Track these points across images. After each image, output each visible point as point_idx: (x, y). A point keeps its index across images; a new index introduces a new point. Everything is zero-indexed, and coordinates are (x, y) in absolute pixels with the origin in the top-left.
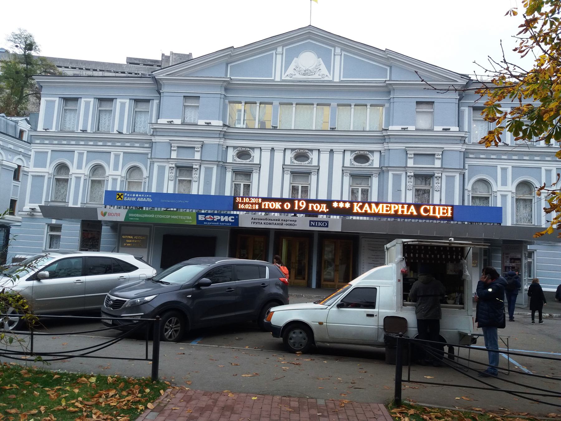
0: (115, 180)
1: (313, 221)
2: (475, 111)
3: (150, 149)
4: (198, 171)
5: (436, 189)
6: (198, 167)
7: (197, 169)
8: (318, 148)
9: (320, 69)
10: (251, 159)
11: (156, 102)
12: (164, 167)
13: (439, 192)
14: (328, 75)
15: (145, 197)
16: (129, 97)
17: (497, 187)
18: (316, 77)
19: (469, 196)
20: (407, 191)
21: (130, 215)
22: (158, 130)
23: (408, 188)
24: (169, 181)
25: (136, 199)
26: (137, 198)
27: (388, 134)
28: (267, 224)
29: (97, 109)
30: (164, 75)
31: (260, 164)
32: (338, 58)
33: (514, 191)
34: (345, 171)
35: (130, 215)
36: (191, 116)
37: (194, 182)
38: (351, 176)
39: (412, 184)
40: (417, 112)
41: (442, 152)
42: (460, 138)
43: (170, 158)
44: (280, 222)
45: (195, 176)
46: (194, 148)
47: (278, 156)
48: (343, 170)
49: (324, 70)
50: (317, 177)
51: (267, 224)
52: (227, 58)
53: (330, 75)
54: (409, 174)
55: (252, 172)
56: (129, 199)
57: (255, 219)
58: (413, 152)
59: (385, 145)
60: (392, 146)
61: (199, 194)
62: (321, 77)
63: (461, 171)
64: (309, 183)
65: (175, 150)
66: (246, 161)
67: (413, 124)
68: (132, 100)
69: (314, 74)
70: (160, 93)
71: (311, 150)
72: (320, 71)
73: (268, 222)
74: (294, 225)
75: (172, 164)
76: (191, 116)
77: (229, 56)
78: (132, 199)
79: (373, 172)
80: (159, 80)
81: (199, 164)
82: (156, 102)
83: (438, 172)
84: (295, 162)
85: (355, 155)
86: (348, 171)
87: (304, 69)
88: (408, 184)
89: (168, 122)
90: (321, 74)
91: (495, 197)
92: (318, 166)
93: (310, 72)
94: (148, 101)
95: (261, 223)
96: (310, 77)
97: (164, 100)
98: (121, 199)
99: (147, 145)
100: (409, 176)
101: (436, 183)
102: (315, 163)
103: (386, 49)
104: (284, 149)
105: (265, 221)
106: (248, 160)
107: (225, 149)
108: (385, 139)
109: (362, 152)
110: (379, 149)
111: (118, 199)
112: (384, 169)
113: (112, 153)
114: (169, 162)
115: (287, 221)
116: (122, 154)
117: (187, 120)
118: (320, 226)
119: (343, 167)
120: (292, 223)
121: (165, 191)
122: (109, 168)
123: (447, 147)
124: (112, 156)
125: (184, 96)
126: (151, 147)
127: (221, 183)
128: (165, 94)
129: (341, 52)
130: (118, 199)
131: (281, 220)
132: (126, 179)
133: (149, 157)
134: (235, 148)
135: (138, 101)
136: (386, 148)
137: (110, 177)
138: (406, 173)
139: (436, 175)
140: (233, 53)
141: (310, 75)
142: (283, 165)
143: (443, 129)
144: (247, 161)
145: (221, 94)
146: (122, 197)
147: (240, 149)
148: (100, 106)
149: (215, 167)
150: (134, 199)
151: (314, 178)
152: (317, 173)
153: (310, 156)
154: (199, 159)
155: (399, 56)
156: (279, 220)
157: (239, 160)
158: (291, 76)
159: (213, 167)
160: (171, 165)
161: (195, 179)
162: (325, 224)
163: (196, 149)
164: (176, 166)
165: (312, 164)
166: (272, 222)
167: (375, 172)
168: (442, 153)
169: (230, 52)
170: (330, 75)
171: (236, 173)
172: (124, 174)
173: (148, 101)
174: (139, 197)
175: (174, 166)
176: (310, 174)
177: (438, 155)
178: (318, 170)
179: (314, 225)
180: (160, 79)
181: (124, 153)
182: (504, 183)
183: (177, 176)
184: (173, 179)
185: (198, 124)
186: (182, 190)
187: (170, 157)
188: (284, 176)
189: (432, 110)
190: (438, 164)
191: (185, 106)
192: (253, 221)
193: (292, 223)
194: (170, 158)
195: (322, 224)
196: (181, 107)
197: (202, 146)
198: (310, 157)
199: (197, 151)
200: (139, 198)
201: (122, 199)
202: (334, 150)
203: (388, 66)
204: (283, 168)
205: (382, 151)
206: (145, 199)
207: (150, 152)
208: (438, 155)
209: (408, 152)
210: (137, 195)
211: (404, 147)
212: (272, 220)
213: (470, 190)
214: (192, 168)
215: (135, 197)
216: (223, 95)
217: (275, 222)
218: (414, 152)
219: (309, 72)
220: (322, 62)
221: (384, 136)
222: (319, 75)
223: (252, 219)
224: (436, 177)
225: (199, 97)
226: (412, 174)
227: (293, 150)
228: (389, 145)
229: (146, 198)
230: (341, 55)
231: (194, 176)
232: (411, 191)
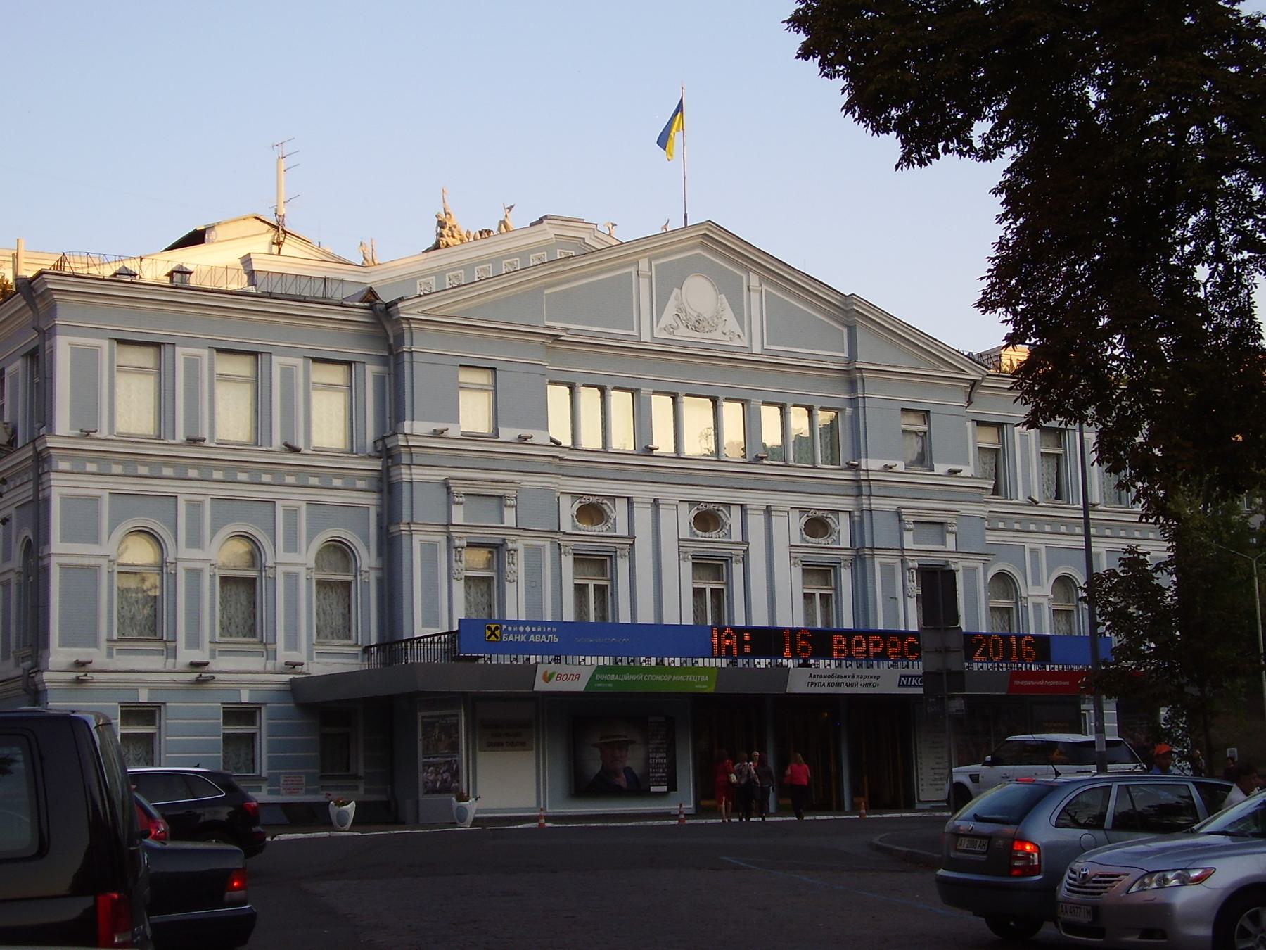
15: (544, 633)
105: (831, 680)
146: (497, 633)
156: (853, 677)
167: (845, 557)
192: (811, 680)
193: (874, 680)
210: (528, 629)
223: (811, 676)
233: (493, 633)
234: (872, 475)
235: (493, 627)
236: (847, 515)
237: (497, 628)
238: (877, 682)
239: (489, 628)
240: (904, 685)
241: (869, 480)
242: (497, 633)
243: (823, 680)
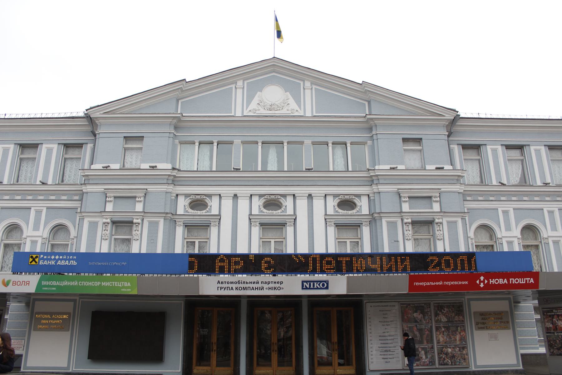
0: (34, 243)
1: (307, 282)
2: (466, 150)
3: (80, 202)
4: (140, 226)
5: (438, 238)
6: (139, 221)
7: (139, 224)
8: (293, 192)
9: (288, 104)
10: (207, 209)
11: (90, 146)
12: (96, 223)
13: (442, 241)
14: (298, 109)
16: (58, 141)
17: (501, 232)
18: (284, 112)
19: (472, 244)
20: (406, 241)
22: (90, 177)
23: (406, 238)
24: (102, 240)
25: (56, 263)
27: (377, 174)
28: (240, 289)
29: (18, 157)
30: (101, 113)
31: (219, 215)
32: (308, 92)
33: (520, 236)
34: (329, 220)
35: (44, 283)
36: (132, 160)
37: (134, 241)
38: (336, 226)
39: (410, 232)
40: (405, 150)
41: (439, 194)
42: (456, 178)
43: (105, 212)
44: (260, 285)
45: (136, 233)
46: (135, 197)
47: (243, 204)
48: (325, 219)
49: (293, 105)
50: (294, 229)
51: (240, 289)
52: (178, 93)
53: (301, 109)
54: (405, 221)
55: (209, 226)
56: (46, 263)
58: (407, 195)
59: (374, 187)
60: (382, 188)
61: (141, 253)
62: (290, 113)
63: (463, 215)
64: (284, 237)
65: (111, 201)
66: (202, 212)
67: (402, 164)
68: (61, 145)
69: (282, 109)
70: (95, 135)
71: (284, 196)
72: (288, 105)
74: (279, 288)
75: (107, 219)
76: (132, 160)
77: (180, 90)
78: (50, 263)
79: (362, 220)
80: (95, 120)
81: (141, 217)
82: (90, 146)
83: (438, 217)
84: (265, 211)
85: (339, 201)
86: (332, 220)
87: (270, 103)
88: (406, 233)
89: (103, 167)
90: (290, 109)
91: (500, 245)
92: (295, 214)
93: (277, 107)
94: (79, 146)
95: (232, 289)
96: (278, 113)
97: (100, 142)
98: (35, 263)
99: (77, 198)
100: (406, 223)
101: (438, 230)
102: (290, 211)
103: (363, 81)
104: (249, 195)
106: (204, 211)
107: (174, 198)
108: (373, 181)
109: (347, 197)
110: (367, 193)
111: (31, 263)
112: (375, 215)
113: (32, 209)
114: (103, 216)
115: (269, 283)
116: (45, 210)
117: (127, 166)
118: (317, 288)
119: (326, 215)
120: (277, 285)
121: (97, 251)
122: (28, 228)
123: (444, 188)
124: (33, 213)
125: (124, 137)
126: (81, 200)
127: (170, 238)
128: (101, 135)
129: (311, 85)
130: (31, 263)
131: (260, 283)
132: (49, 241)
133: (79, 211)
134: (187, 196)
135: (69, 147)
136: (375, 190)
137: (28, 239)
138: (402, 220)
139: (437, 221)
140: (184, 88)
141: (277, 110)
142: (249, 215)
143: (391, 168)
144: (203, 212)
145: (170, 133)
147: (194, 198)
148: (22, 153)
149: (162, 220)
150: (53, 263)
151: (290, 230)
152: (294, 224)
153: (282, 202)
154: (141, 210)
155: (378, 90)
156: (258, 283)
157: (193, 211)
158: (255, 111)
159: (159, 221)
160: (105, 220)
161: (136, 238)
162: (323, 285)
163: (137, 199)
164: (111, 221)
165: (286, 213)
167: (365, 220)
168: (440, 195)
169: (182, 86)
170: (301, 109)
171: (189, 227)
172: (46, 235)
173: (79, 146)
174: (59, 259)
175: (109, 221)
176: (285, 225)
177: (435, 197)
178: (295, 219)
179: (308, 286)
180: (96, 118)
181: (48, 208)
182: (508, 228)
183: (113, 234)
184: (107, 238)
185: (141, 168)
186: (121, 249)
187: (105, 210)
188: (251, 229)
189: (420, 148)
190: (436, 207)
191: (126, 149)
193: (277, 285)
194: (105, 212)
195: (319, 285)
196: (121, 151)
197: (145, 194)
198: (284, 204)
199: (138, 201)
202: (313, 195)
203: (366, 101)
204: (250, 219)
205: (370, 195)
206: (67, 261)
207: (80, 205)
208: (435, 197)
209: (401, 194)
211: (397, 189)
212: (247, 283)
213: (472, 238)
214: (132, 222)
215: (55, 259)
216: (172, 134)
217: (251, 286)
218: (407, 194)
219: (276, 107)
220: (290, 96)
221: (371, 176)
222: (288, 110)
224: (437, 223)
225: (143, 137)
226: (410, 221)
227: (261, 196)
228: (379, 187)
229: (69, 260)
230: (312, 89)
231: (134, 233)
232: (411, 241)
233: (34, 260)
234: (378, 172)
235: (34, 256)
236: (367, 198)
237: (37, 257)
238: (282, 286)
239: (32, 257)
240: (306, 288)
241: (377, 176)
242: (37, 260)
243: (230, 286)
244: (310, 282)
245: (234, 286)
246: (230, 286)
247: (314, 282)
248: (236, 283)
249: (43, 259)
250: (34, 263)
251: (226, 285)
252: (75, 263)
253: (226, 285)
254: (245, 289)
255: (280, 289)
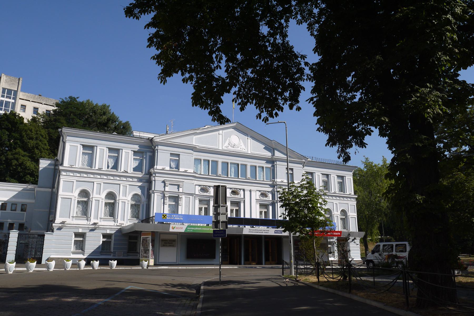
21: (188, 228)
26: (175, 217)
44: (262, 231)
57: (250, 230)
73: (256, 231)
105: (255, 231)
120: (267, 231)
156: (262, 230)
166: (259, 231)
192: (250, 231)
193: (267, 231)
200: (175, 218)
201: (165, 218)
217: (259, 231)
223: (249, 230)
233: (164, 217)
235: (164, 215)
237: (165, 215)
239: (163, 215)
242: (166, 217)
243: (253, 231)
244: (277, 231)
245: (254, 231)
246: (253, 231)
247: (278, 231)
248: (255, 230)
249: (168, 216)
250: (164, 218)
251: (252, 231)
252: (182, 219)
253: (252, 231)
254: (257, 232)
255: (268, 233)
